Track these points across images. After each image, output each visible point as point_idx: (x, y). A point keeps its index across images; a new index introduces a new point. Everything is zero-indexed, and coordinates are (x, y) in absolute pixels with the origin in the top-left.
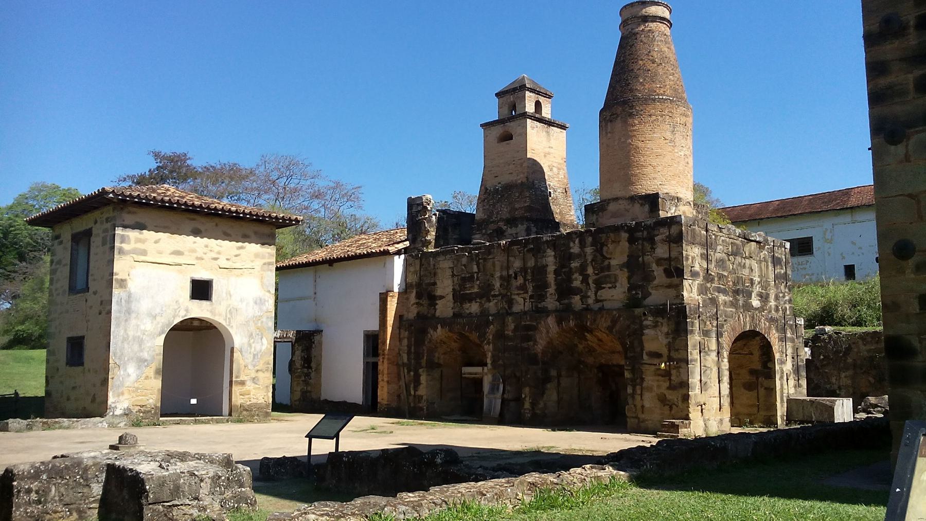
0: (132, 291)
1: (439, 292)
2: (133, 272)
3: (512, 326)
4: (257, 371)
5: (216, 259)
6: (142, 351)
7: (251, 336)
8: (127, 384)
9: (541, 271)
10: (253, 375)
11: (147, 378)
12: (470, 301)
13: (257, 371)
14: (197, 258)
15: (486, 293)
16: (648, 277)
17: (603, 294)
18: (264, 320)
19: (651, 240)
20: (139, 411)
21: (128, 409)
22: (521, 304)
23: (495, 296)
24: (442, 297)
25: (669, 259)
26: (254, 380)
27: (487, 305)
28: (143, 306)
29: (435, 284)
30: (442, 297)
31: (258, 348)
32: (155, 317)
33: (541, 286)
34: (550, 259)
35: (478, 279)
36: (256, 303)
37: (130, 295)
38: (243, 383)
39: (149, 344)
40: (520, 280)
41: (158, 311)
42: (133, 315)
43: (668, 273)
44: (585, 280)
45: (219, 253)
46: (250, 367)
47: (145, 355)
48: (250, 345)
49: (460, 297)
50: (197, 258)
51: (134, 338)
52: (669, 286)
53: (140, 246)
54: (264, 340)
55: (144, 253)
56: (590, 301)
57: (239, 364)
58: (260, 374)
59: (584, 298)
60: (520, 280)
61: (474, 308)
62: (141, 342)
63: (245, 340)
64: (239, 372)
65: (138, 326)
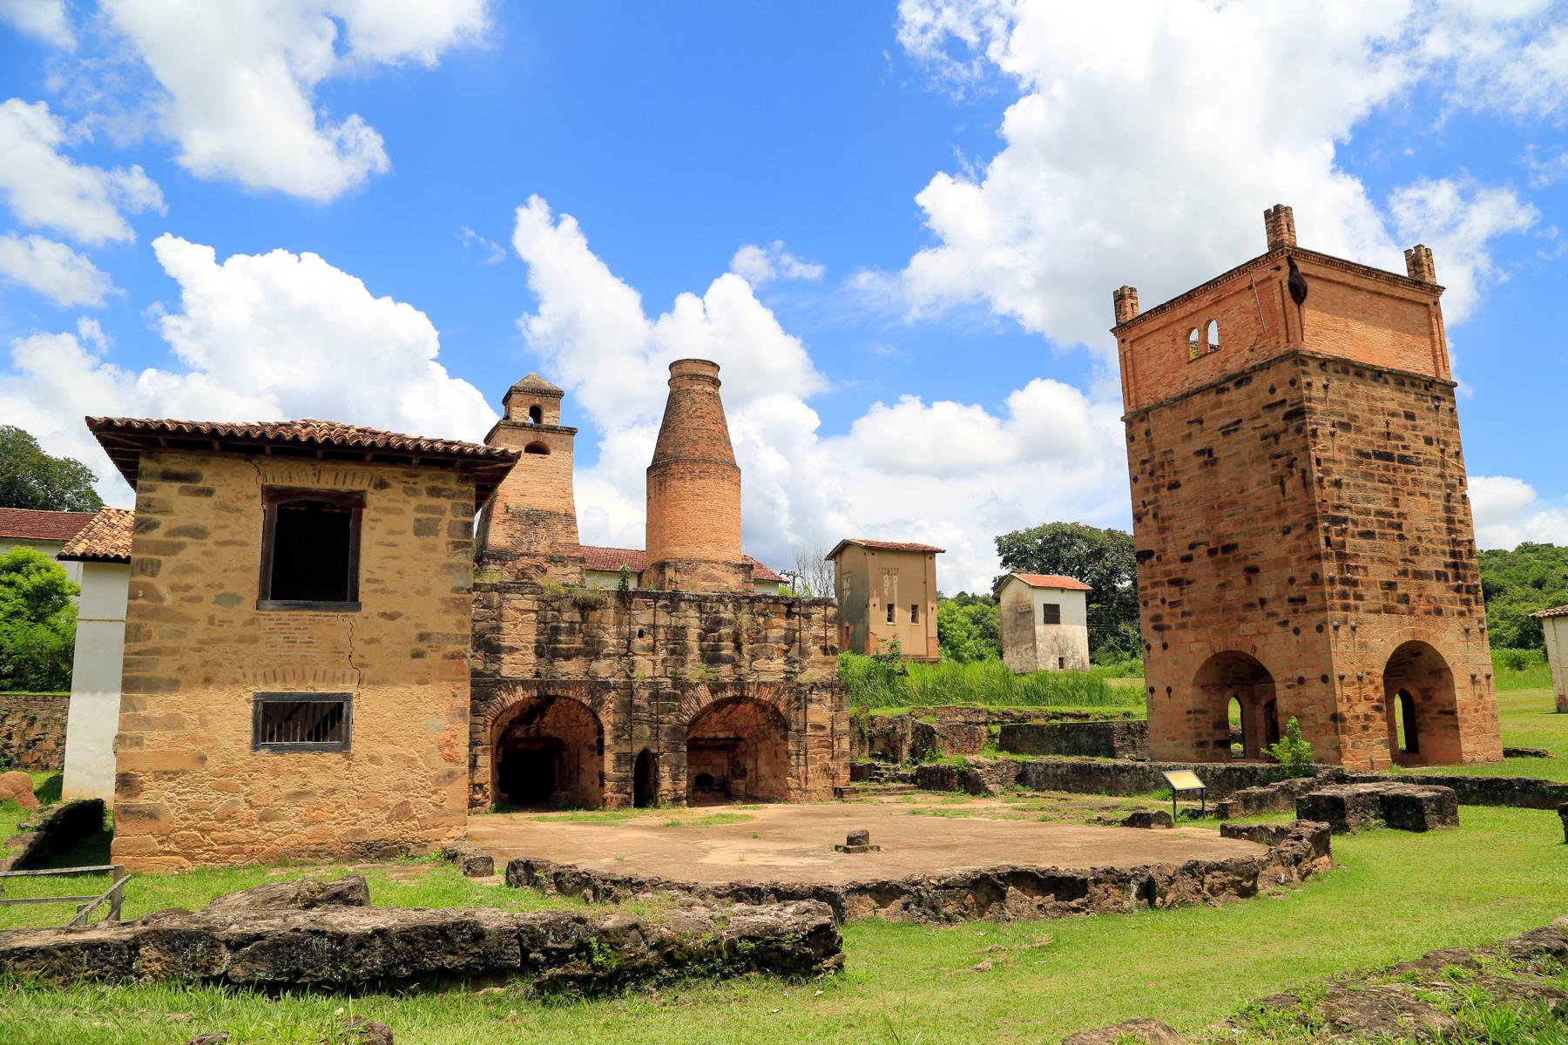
1: (506, 643)
3: (645, 694)
9: (678, 633)
12: (567, 658)
15: (592, 651)
16: (803, 652)
17: (761, 664)
19: (808, 616)
22: (645, 667)
23: (608, 656)
24: (512, 650)
25: (825, 638)
27: (595, 665)
29: (498, 629)
30: (512, 650)
33: (678, 651)
34: (693, 623)
35: (581, 631)
40: (648, 640)
43: (825, 650)
44: (738, 648)
49: (547, 649)
52: (825, 663)
56: (744, 670)
59: (736, 666)
60: (648, 640)
61: (571, 669)
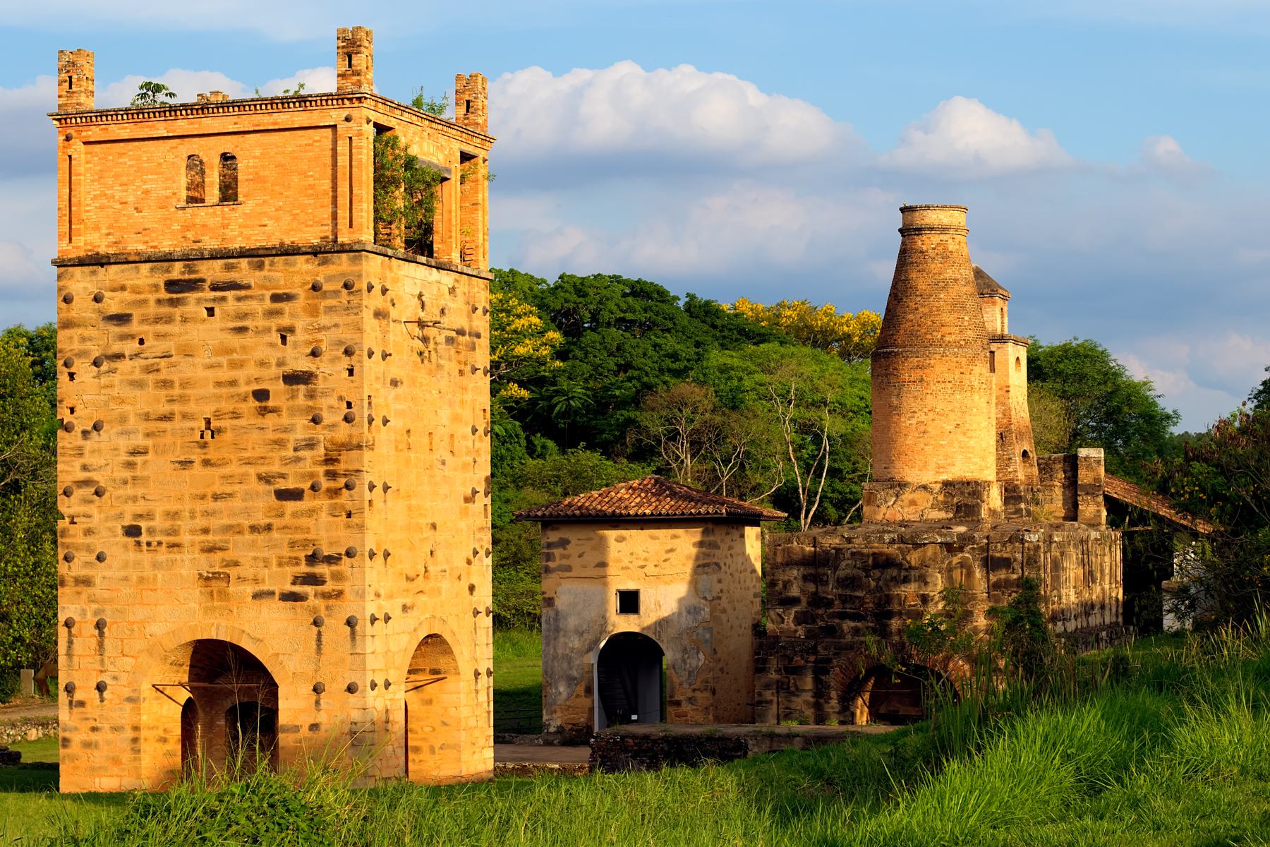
0: (560, 608)
2: (559, 589)
4: (694, 690)
5: (643, 567)
6: (571, 669)
7: (685, 650)
8: (559, 702)
10: (690, 694)
11: (578, 696)
13: (694, 690)
14: (623, 568)
18: (700, 631)
20: (572, 729)
21: (561, 726)
26: (691, 700)
28: (572, 622)
31: (694, 663)
32: (582, 634)
36: (689, 612)
37: (557, 613)
38: (678, 703)
39: (577, 662)
41: (585, 627)
42: (562, 633)
45: (646, 559)
46: (685, 685)
47: (575, 673)
48: (684, 661)
50: (623, 568)
51: (564, 656)
53: (565, 562)
54: (701, 656)
55: (569, 569)
57: (672, 682)
58: (698, 694)
62: (569, 660)
63: (679, 656)
64: (673, 688)
65: (566, 644)
